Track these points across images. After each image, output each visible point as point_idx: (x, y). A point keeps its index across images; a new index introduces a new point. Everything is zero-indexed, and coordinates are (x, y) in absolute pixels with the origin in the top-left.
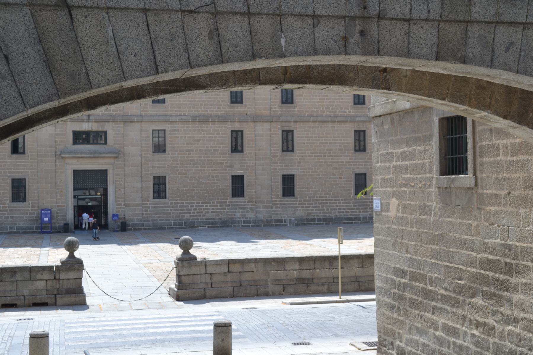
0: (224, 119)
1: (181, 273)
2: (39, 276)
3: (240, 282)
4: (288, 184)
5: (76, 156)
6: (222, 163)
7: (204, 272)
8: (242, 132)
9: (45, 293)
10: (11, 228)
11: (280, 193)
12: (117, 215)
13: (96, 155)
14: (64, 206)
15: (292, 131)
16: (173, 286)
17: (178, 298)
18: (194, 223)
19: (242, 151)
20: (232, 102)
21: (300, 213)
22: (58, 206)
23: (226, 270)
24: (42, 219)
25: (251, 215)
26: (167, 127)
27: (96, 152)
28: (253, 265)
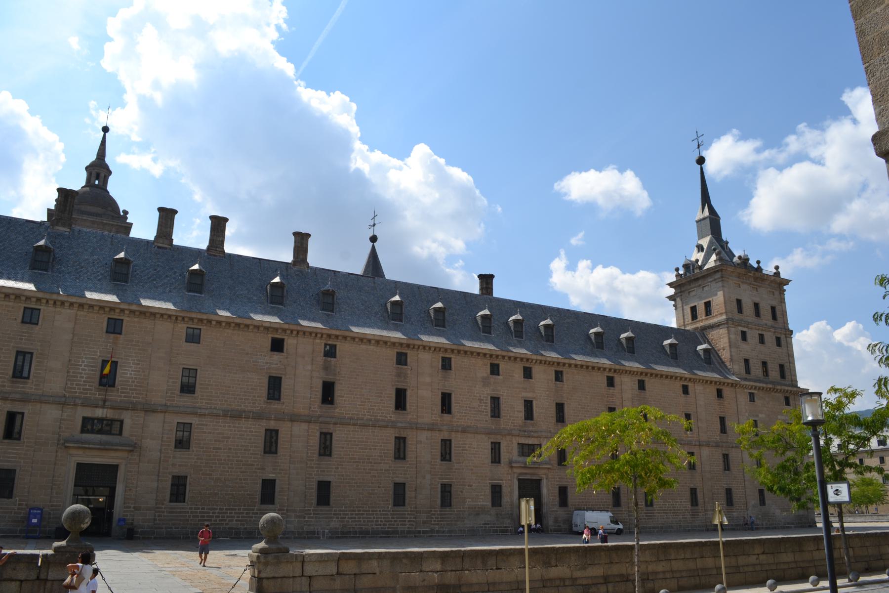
0: (258, 416)
1: (263, 575)
4: (324, 491)
6: (253, 465)
7: (298, 572)
11: (314, 501)
12: (124, 520)
13: (107, 447)
14: (60, 506)
15: (331, 434)
19: (276, 453)
21: (335, 524)
22: (52, 506)
23: (334, 571)
24: (29, 520)
26: (194, 420)
28: (375, 563)
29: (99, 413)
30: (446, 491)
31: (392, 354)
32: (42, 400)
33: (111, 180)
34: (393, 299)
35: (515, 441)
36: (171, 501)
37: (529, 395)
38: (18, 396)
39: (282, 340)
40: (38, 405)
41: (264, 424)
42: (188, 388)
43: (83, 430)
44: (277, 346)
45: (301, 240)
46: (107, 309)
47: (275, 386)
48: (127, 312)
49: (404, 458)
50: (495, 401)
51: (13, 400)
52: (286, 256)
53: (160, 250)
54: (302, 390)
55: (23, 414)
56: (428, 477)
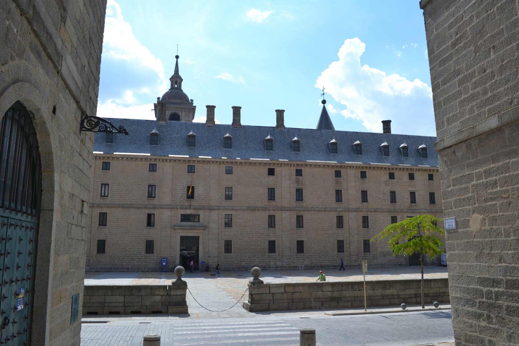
0: (264, 209)
1: (253, 293)
2: (157, 292)
3: (293, 299)
5: (182, 228)
7: (268, 292)
8: (274, 216)
9: (160, 304)
10: (145, 268)
11: (296, 251)
12: (204, 262)
15: (302, 216)
16: (247, 302)
17: (251, 310)
18: (247, 268)
19: (274, 227)
20: (269, 200)
21: (307, 262)
23: (283, 291)
24: (162, 263)
25: (279, 263)
26: (233, 213)
27: (194, 226)
28: (301, 288)
29: (188, 212)
30: (367, 245)
31: (333, 172)
32: (162, 207)
33: (183, 83)
34: (331, 142)
36: (225, 253)
37: (412, 189)
38: (151, 206)
39: (274, 169)
40: (161, 210)
41: (268, 213)
42: (229, 197)
43: (182, 220)
44: (271, 172)
45: (280, 114)
46: (187, 161)
47: (271, 194)
48: (196, 162)
49: (342, 227)
50: (393, 194)
51: (149, 208)
52: (273, 123)
53: (209, 128)
54: (286, 193)
55: (154, 214)
56: (356, 236)
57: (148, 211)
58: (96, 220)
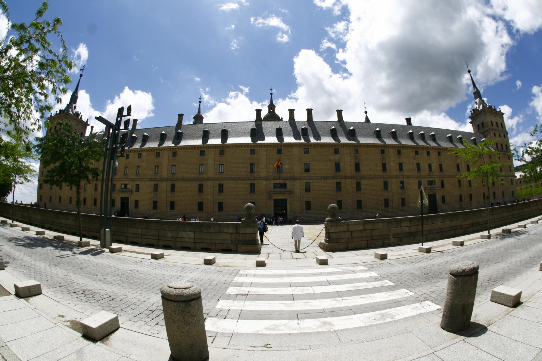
0: (333, 178)
1: (330, 231)
7: (346, 229)
9: (230, 242)
16: (323, 241)
26: (311, 181)
28: (380, 224)
29: (278, 181)
32: (260, 179)
33: (276, 109)
35: (426, 180)
37: (429, 162)
42: (307, 170)
43: (275, 187)
47: (338, 167)
50: (418, 165)
51: (251, 180)
57: (250, 182)
58: (217, 189)
